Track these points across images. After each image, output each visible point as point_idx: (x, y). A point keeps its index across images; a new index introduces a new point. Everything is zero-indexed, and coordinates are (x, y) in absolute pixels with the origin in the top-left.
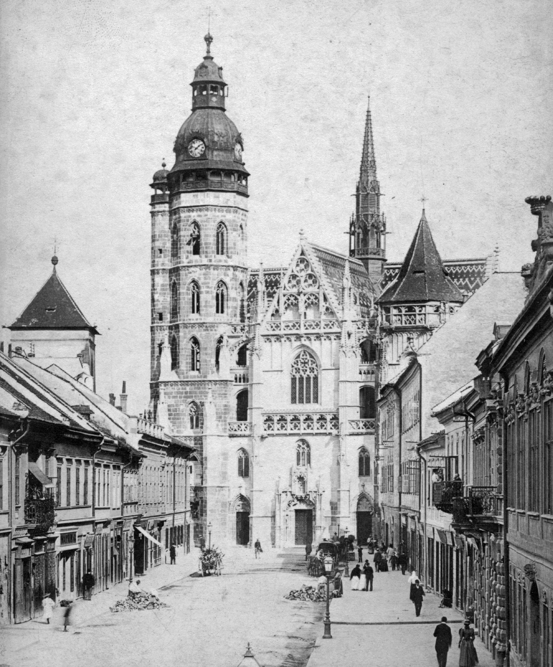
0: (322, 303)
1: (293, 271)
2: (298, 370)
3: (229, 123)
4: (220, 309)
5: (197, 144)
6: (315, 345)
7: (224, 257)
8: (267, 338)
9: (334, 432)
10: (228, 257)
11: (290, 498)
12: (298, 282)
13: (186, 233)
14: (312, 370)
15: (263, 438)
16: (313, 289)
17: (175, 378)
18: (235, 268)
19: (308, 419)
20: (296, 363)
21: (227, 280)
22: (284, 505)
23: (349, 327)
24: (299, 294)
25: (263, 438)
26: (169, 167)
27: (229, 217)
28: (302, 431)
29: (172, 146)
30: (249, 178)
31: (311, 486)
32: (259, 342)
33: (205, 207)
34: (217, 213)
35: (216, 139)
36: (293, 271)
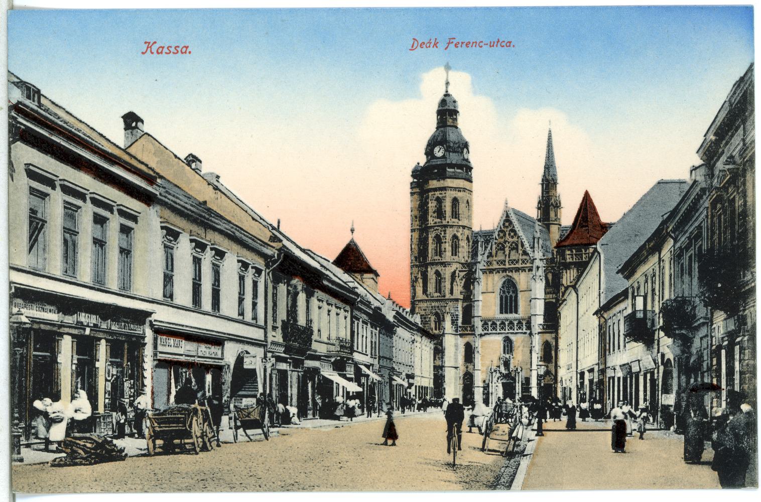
0: (520, 247)
1: (501, 228)
2: (504, 292)
3: (460, 135)
4: (455, 252)
6: (515, 275)
7: (456, 220)
8: (484, 272)
9: (528, 332)
10: (459, 220)
11: (498, 375)
12: (505, 235)
13: (432, 205)
14: (513, 292)
15: (481, 335)
16: (515, 239)
17: (425, 297)
18: (464, 227)
19: (511, 323)
20: (503, 287)
21: (459, 235)
22: (495, 380)
23: (537, 263)
24: (505, 242)
25: (481, 335)
26: (422, 164)
27: (459, 195)
28: (507, 331)
29: (424, 152)
30: (473, 170)
31: (512, 367)
32: (479, 274)
33: (444, 189)
34: (452, 192)
35: (452, 145)
36: (501, 228)
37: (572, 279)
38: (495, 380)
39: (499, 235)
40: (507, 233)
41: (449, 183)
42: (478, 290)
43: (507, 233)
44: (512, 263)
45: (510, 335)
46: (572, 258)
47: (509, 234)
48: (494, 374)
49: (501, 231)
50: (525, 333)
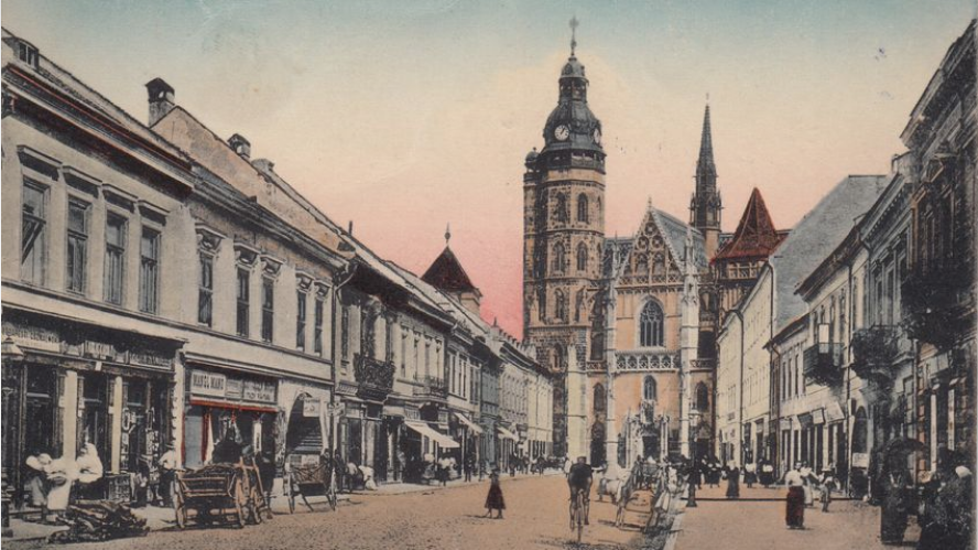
0: (667, 258)
3: (588, 112)
4: (581, 265)
5: (558, 131)
6: (661, 297)
7: (583, 224)
8: (620, 291)
9: (677, 370)
10: (588, 223)
11: (638, 426)
12: (648, 243)
13: (552, 204)
14: (658, 318)
15: (616, 375)
16: (661, 249)
17: (542, 324)
18: (594, 233)
19: (655, 358)
20: (645, 311)
21: (587, 242)
23: (690, 280)
24: (648, 252)
25: (616, 375)
26: (539, 150)
27: (588, 190)
28: (650, 369)
29: (542, 133)
31: (655, 415)
32: (613, 294)
33: (568, 182)
34: (579, 187)
35: (578, 124)
37: (735, 301)
38: (633, 433)
39: (640, 243)
40: (651, 241)
41: (575, 174)
42: (612, 315)
43: (651, 241)
44: (657, 279)
45: (654, 375)
46: (736, 274)
47: (653, 242)
48: (632, 425)
49: (643, 238)
50: (673, 372)
